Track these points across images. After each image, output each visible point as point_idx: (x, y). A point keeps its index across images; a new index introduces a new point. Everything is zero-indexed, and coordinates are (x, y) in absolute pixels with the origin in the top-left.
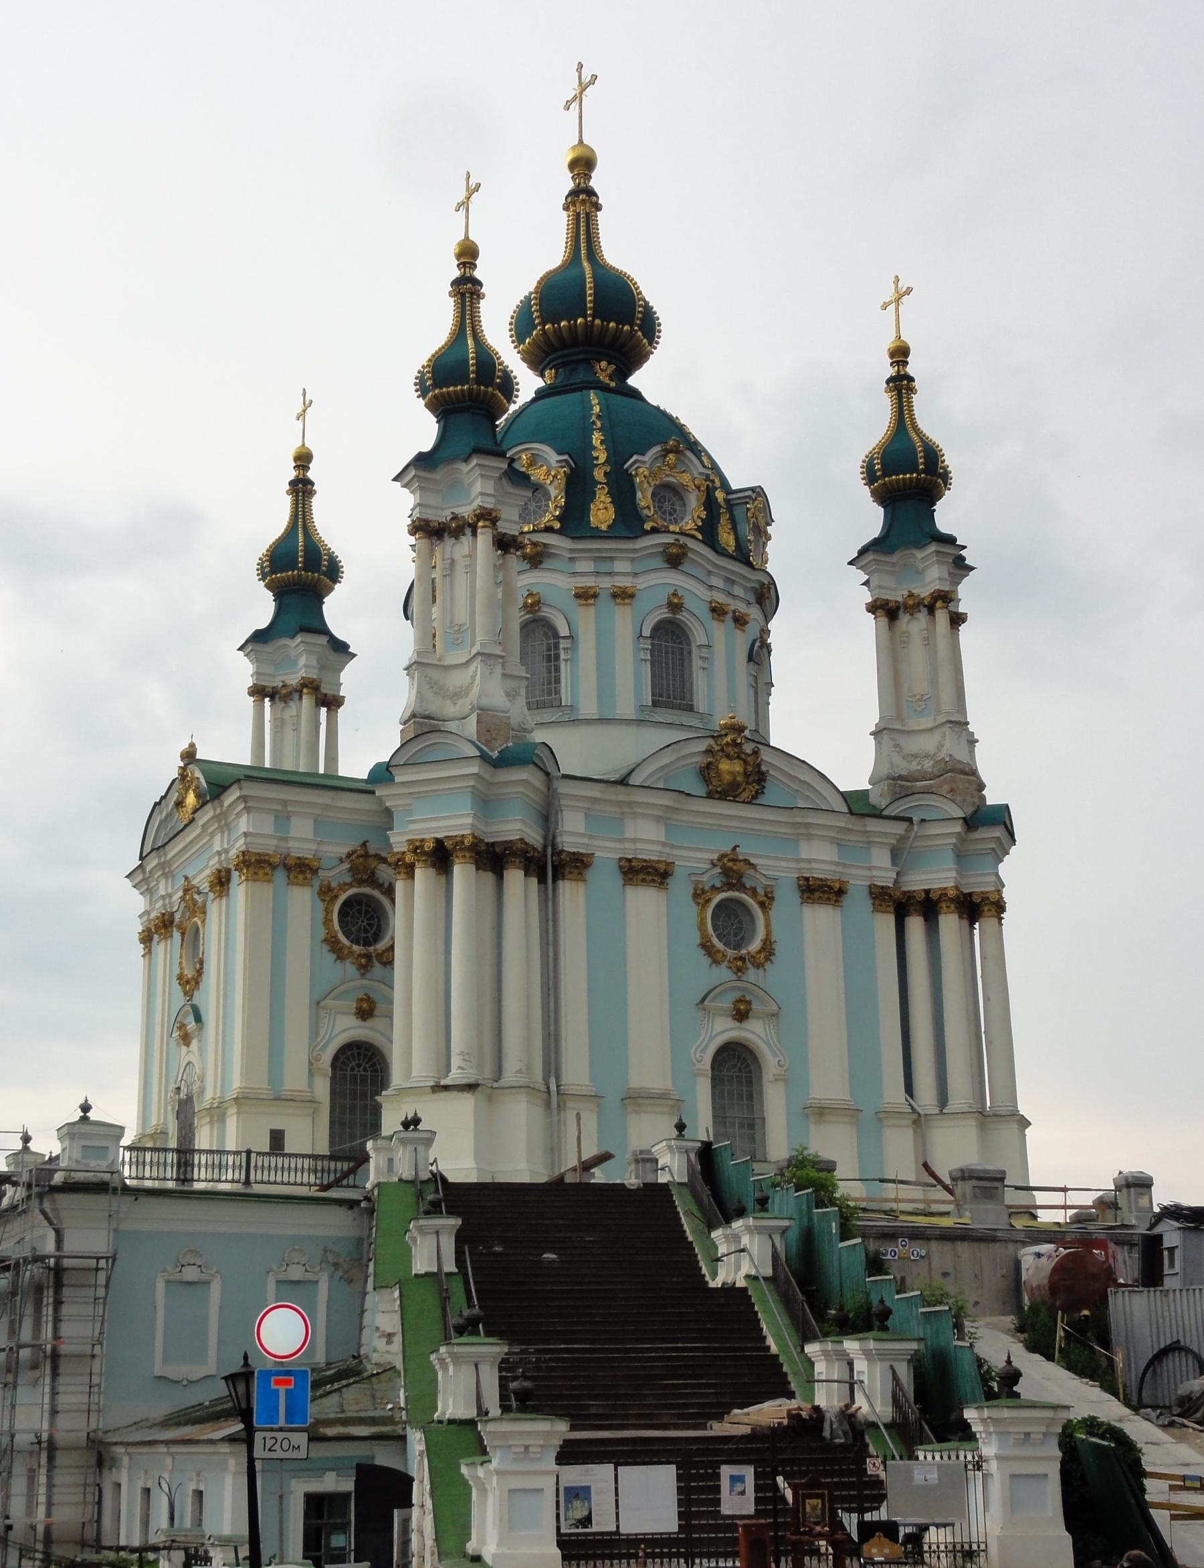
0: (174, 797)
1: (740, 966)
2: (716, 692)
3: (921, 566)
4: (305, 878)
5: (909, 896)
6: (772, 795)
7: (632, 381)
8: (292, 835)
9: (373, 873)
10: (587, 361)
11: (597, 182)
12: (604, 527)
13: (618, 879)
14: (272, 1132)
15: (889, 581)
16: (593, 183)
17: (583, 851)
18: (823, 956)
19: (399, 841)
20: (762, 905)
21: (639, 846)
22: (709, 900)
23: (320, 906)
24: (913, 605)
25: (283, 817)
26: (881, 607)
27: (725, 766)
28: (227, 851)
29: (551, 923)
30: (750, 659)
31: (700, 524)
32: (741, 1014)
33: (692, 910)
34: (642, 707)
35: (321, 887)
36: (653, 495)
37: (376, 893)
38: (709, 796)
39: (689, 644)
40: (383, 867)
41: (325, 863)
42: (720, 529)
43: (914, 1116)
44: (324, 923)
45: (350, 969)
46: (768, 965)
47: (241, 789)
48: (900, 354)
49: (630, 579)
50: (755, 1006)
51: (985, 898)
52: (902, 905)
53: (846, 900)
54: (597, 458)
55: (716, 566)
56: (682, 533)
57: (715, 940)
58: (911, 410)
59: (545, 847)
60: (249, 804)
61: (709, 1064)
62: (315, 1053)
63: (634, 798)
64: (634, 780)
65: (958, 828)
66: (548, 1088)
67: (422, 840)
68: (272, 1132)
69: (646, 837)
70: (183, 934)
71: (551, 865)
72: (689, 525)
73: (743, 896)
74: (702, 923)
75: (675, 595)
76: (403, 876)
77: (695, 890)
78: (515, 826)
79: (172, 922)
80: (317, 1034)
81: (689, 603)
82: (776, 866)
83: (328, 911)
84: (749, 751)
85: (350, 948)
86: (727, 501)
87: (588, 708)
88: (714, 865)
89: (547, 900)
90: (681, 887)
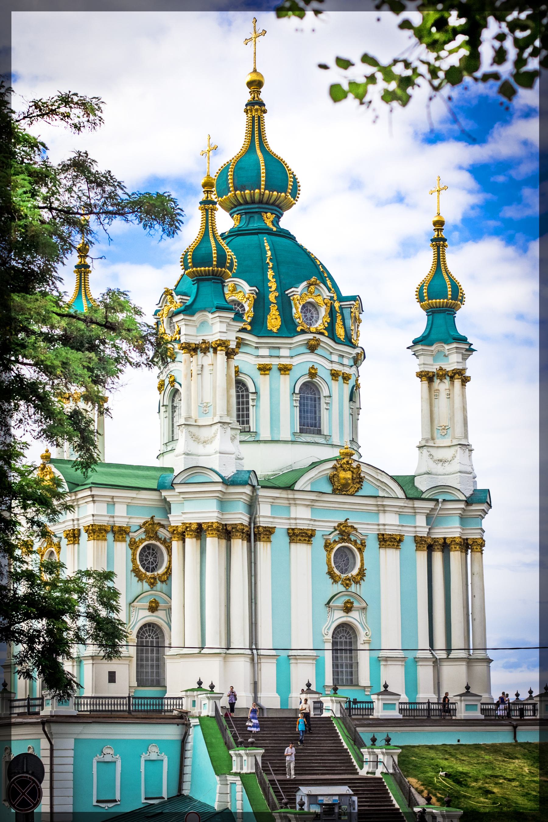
1: (347, 583)
3: (447, 353)
5: (435, 540)
6: (366, 490)
9: (156, 533)
10: (259, 213)
11: (264, 95)
12: (275, 330)
13: (287, 539)
14: (109, 672)
15: (430, 360)
16: (261, 97)
17: (270, 526)
18: (389, 575)
20: (360, 550)
22: (333, 548)
23: (130, 552)
24: (442, 375)
25: (112, 503)
26: (425, 376)
27: (342, 474)
30: (351, 399)
31: (327, 326)
32: (348, 608)
34: (294, 434)
35: (130, 542)
36: (302, 309)
37: (158, 544)
38: (334, 492)
40: (162, 530)
41: (133, 529)
42: (337, 326)
43: (434, 660)
44: (133, 562)
45: (146, 586)
47: (91, 491)
49: (289, 359)
50: (356, 604)
51: (475, 541)
54: (271, 287)
55: (335, 349)
59: (250, 523)
64: (297, 487)
65: (462, 506)
68: (109, 672)
69: (302, 516)
71: (255, 534)
72: (320, 324)
73: (350, 545)
74: (329, 561)
76: (176, 539)
77: (326, 543)
78: (238, 516)
81: (321, 372)
82: (367, 528)
83: (134, 554)
84: (355, 466)
85: (145, 574)
86: (341, 308)
87: (265, 434)
88: (336, 530)
89: (251, 552)
90: (318, 541)
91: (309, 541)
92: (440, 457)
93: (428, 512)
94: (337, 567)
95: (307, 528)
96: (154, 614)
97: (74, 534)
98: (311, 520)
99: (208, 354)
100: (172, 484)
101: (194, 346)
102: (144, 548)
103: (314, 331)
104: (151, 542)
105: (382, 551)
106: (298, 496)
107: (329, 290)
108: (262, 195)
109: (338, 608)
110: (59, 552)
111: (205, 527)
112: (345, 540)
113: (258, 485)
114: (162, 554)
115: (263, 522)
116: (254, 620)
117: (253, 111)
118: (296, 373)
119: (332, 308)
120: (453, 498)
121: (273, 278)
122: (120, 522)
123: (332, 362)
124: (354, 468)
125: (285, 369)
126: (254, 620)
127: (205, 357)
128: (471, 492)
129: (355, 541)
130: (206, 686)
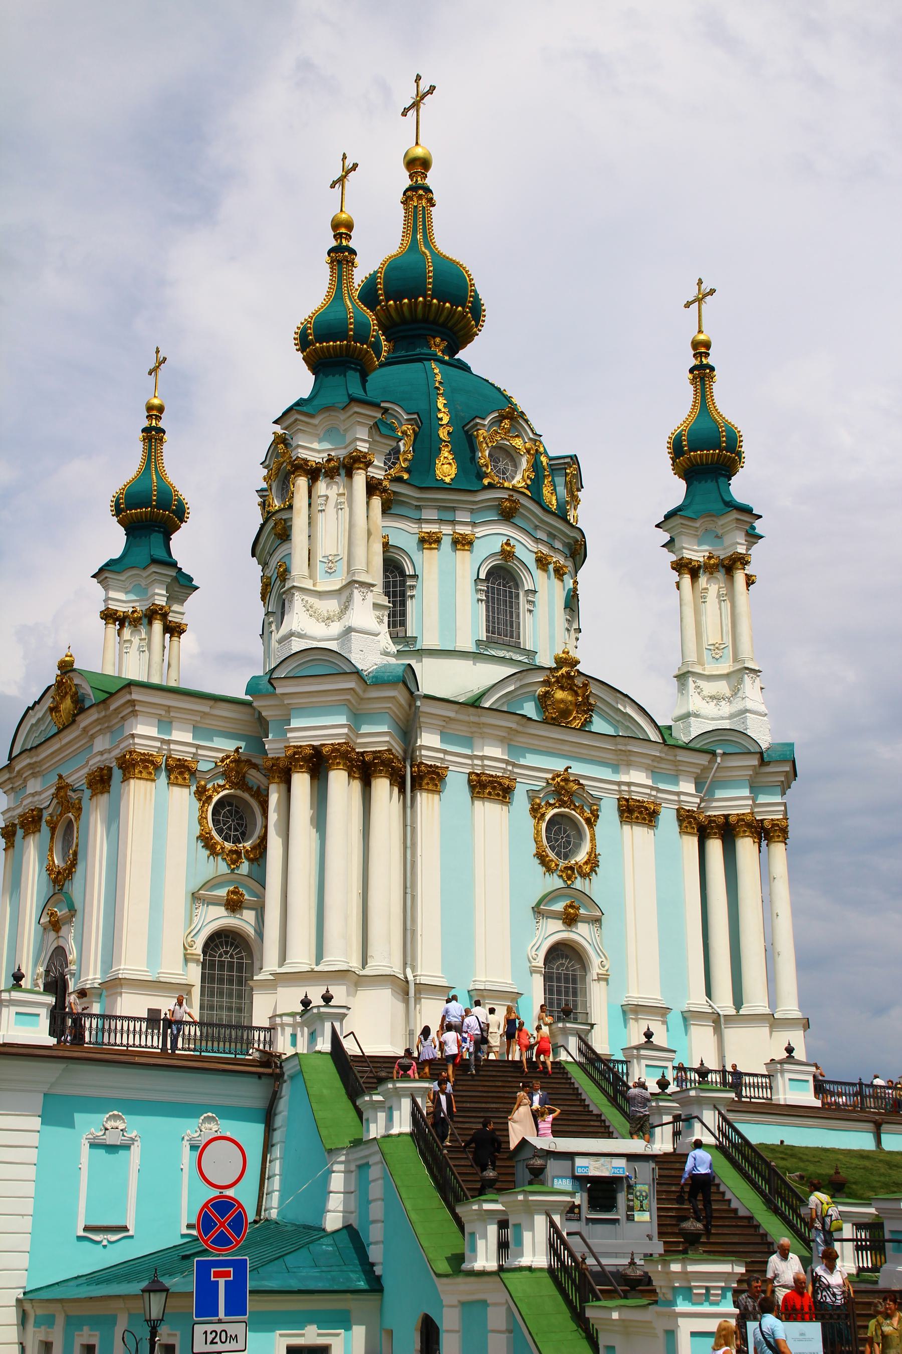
0: (48, 702)
1: (570, 872)
2: (542, 632)
3: (720, 532)
6: (599, 725)
9: (244, 777)
11: (431, 180)
12: (447, 480)
16: (430, 182)
17: (439, 764)
19: (273, 746)
20: (588, 821)
21: (486, 762)
23: (198, 805)
27: (560, 695)
28: (109, 751)
32: (570, 919)
33: (530, 822)
34: (479, 642)
37: (246, 796)
38: (545, 721)
39: (517, 587)
40: (253, 772)
43: (715, 1016)
45: (223, 867)
48: (701, 348)
52: (702, 827)
54: (441, 419)
55: (542, 521)
57: (549, 851)
60: (137, 708)
61: (541, 964)
62: (189, 939)
63: (484, 720)
66: (406, 978)
67: (301, 747)
69: (492, 754)
70: (53, 830)
74: (538, 832)
75: (508, 544)
76: (276, 780)
79: (40, 818)
80: (191, 921)
81: (520, 552)
83: (202, 810)
93: (699, 771)
94: (552, 848)
97: (102, 777)
98: (507, 762)
100: (270, 678)
101: (314, 465)
105: (627, 828)
108: (427, 305)
109: (554, 915)
110: (78, 818)
111: (325, 750)
112: (565, 802)
115: (428, 758)
117: (415, 199)
120: (738, 751)
122: (181, 752)
123: (537, 540)
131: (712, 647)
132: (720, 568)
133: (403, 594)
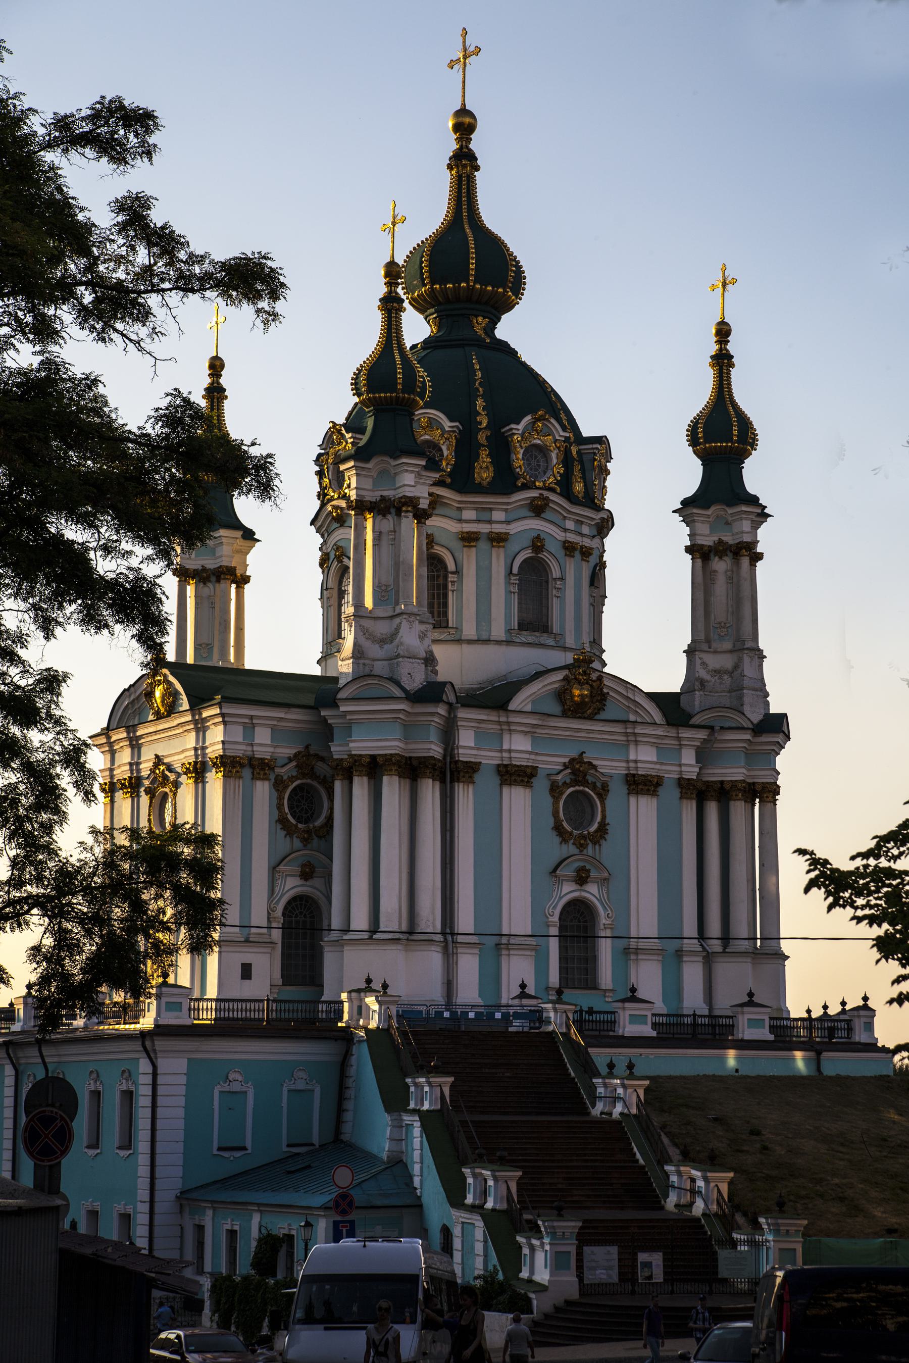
3: (730, 519)
4: (265, 774)
5: (708, 784)
7: (502, 331)
8: (256, 741)
9: (313, 768)
12: (485, 483)
13: (497, 780)
17: (472, 760)
19: (337, 750)
23: (275, 794)
25: (250, 727)
29: (448, 814)
30: (592, 583)
32: (582, 878)
33: (550, 800)
34: (509, 631)
37: (315, 784)
38: (565, 714)
40: (320, 764)
41: (280, 762)
43: (704, 954)
45: (297, 843)
46: (603, 842)
49: (504, 526)
50: (594, 874)
53: (661, 791)
54: (480, 423)
56: (545, 488)
58: (729, 384)
59: (445, 756)
63: (511, 719)
64: (512, 706)
67: (360, 755)
69: (519, 747)
71: (452, 772)
73: (587, 789)
75: (538, 537)
82: (610, 766)
83: (280, 798)
84: (594, 678)
85: (296, 826)
86: (579, 452)
87: (469, 630)
90: (541, 784)
91: (528, 782)
92: (717, 666)
93: (699, 744)
95: (525, 764)
96: (308, 883)
99: (389, 517)
101: (368, 504)
102: (294, 789)
103: (541, 484)
104: (304, 781)
105: (633, 800)
106: (513, 719)
107: (564, 429)
109: (568, 879)
111: (379, 760)
113: (457, 703)
114: (321, 797)
116: (448, 893)
118: (513, 546)
119: (567, 452)
120: (734, 725)
121: (483, 410)
123: (565, 530)
124: (594, 681)
125: (498, 539)
126: (448, 893)
127: (385, 521)
128: (761, 717)
129: (595, 783)
130: (377, 985)
131: (717, 626)
132: (729, 553)
133: (445, 587)
